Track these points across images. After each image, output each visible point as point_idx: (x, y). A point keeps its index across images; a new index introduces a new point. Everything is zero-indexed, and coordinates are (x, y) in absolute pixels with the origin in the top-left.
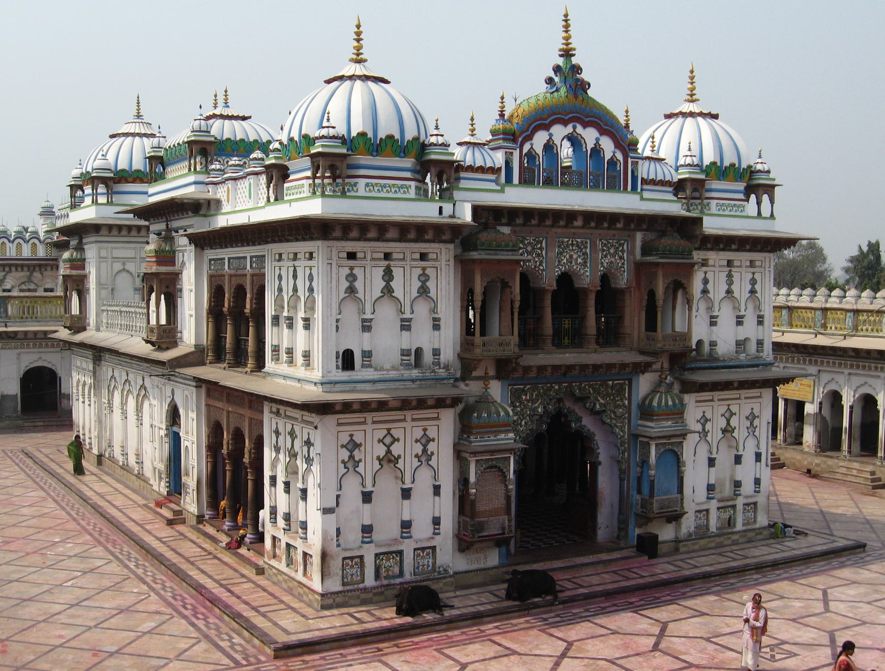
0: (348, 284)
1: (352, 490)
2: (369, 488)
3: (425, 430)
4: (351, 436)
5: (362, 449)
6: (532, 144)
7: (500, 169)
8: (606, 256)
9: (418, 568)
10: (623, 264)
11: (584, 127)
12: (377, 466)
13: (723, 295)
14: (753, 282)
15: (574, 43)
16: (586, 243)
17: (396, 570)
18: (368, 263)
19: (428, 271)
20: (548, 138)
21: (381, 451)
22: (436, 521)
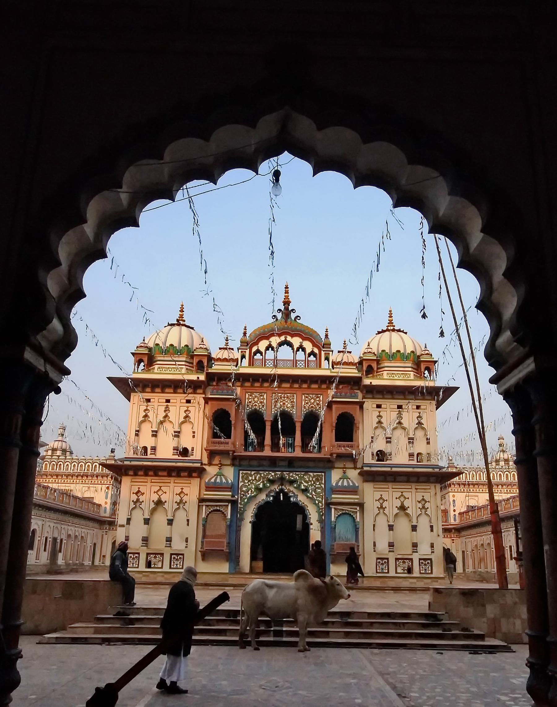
1: (138, 517)
3: (182, 489)
5: (144, 495)
8: (307, 403)
9: (173, 565)
10: (320, 407)
11: (292, 337)
12: (152, 505)
17: (160, 566)
18: (156, 404)
21: (155, 498)
22: (187, 540)
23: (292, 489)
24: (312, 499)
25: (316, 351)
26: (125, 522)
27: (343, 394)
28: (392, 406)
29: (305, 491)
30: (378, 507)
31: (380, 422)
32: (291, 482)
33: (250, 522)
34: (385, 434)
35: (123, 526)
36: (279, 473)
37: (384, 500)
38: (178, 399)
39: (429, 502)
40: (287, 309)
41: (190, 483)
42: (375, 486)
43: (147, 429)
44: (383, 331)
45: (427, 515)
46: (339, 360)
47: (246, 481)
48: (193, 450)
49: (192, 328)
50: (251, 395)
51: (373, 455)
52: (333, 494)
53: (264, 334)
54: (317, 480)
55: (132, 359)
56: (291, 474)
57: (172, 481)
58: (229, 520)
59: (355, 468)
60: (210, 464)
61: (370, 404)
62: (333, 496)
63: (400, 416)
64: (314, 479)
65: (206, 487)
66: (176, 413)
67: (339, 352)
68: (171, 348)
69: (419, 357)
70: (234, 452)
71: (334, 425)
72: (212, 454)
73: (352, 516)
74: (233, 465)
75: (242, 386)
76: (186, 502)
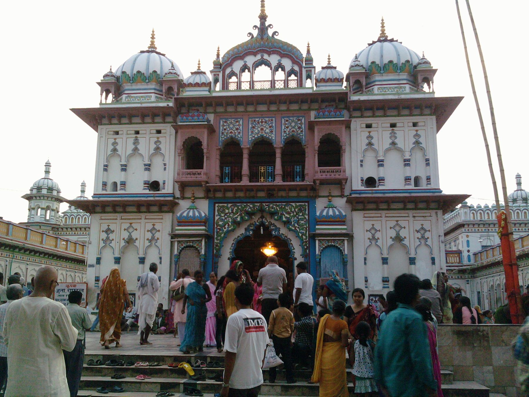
0: (113, 147)
2: (117, 255)
3: (154, 225)
4: (108, 226)
5: (114, 233)
6: (232, 68)
7: (210, 83)
8: (287, 127)
10: (302, 131)
11: (269, 55)
12: (123, 243)
13: (387, 145)
14: (417, 135)
15: (267, 12)
16: (272, 120)
18: (124, 137)
19: (160, 139)
20: (243, 64)
21: (126, 235)
23: (273, 221)
24: (295, 231)
25: (296, 68)
26: (94, 262)
27: (327, 113)
28: (384, 125)
29: (287, 223)
30: (369, 239)
31: (370, 144)
32: (272, 214)
33: (229, 259)
34: (376, 157)
35: (91, 266)
36: (258, 204)
37: (376, 231)
38: (147, 130)
39: (429, 231)
40: (263, 23)
41: (162, 219)
42: (366, 215)
43: (115, 164)
44: (374, 43)
45: (427, 245)
46: (322, 76)
47: (223, 215)
48: (164, 184)
49: (164, 55)
50: (226, 122)
51: (362, 180)
52: (318, 225)
53: (238, 54)
54: (300, 210)
55: (99, 88)
56: (271, 205)
57: (143, 218)
58: (203, 257)
59: (342, 196)
60: (183, 198)
61: (357, 124)
62: (317, 227)
63: (393, 135)
64: (296, 210)
65: (179, 222)
66: (146, 145)
67: (323, 68)
68: (139, 75)
69: (415, 67)
70: (207, 182)
71: (316, 148)
72: (183, 186)
73: (339, 248)
74: (206, 197)
75: (215, 112)
76: (158, 239)
